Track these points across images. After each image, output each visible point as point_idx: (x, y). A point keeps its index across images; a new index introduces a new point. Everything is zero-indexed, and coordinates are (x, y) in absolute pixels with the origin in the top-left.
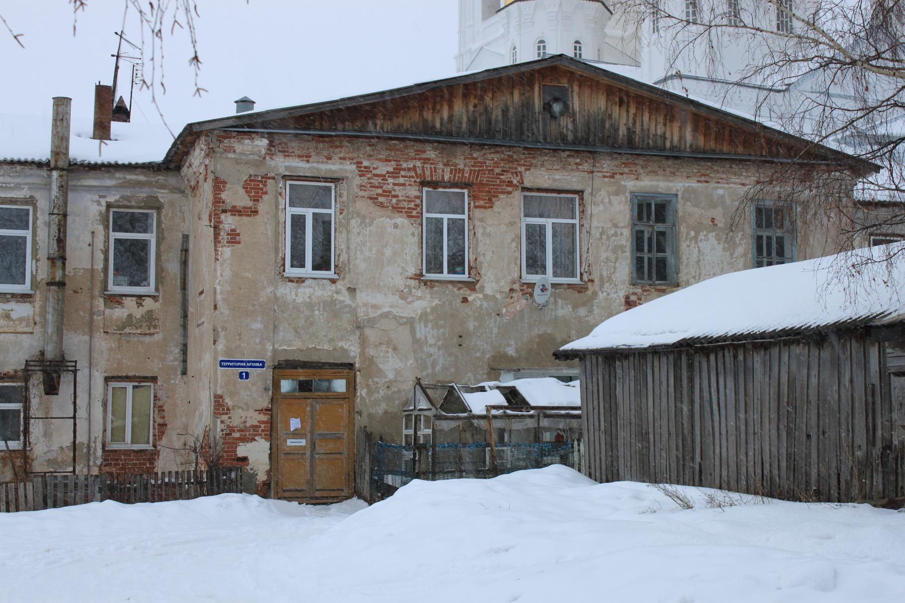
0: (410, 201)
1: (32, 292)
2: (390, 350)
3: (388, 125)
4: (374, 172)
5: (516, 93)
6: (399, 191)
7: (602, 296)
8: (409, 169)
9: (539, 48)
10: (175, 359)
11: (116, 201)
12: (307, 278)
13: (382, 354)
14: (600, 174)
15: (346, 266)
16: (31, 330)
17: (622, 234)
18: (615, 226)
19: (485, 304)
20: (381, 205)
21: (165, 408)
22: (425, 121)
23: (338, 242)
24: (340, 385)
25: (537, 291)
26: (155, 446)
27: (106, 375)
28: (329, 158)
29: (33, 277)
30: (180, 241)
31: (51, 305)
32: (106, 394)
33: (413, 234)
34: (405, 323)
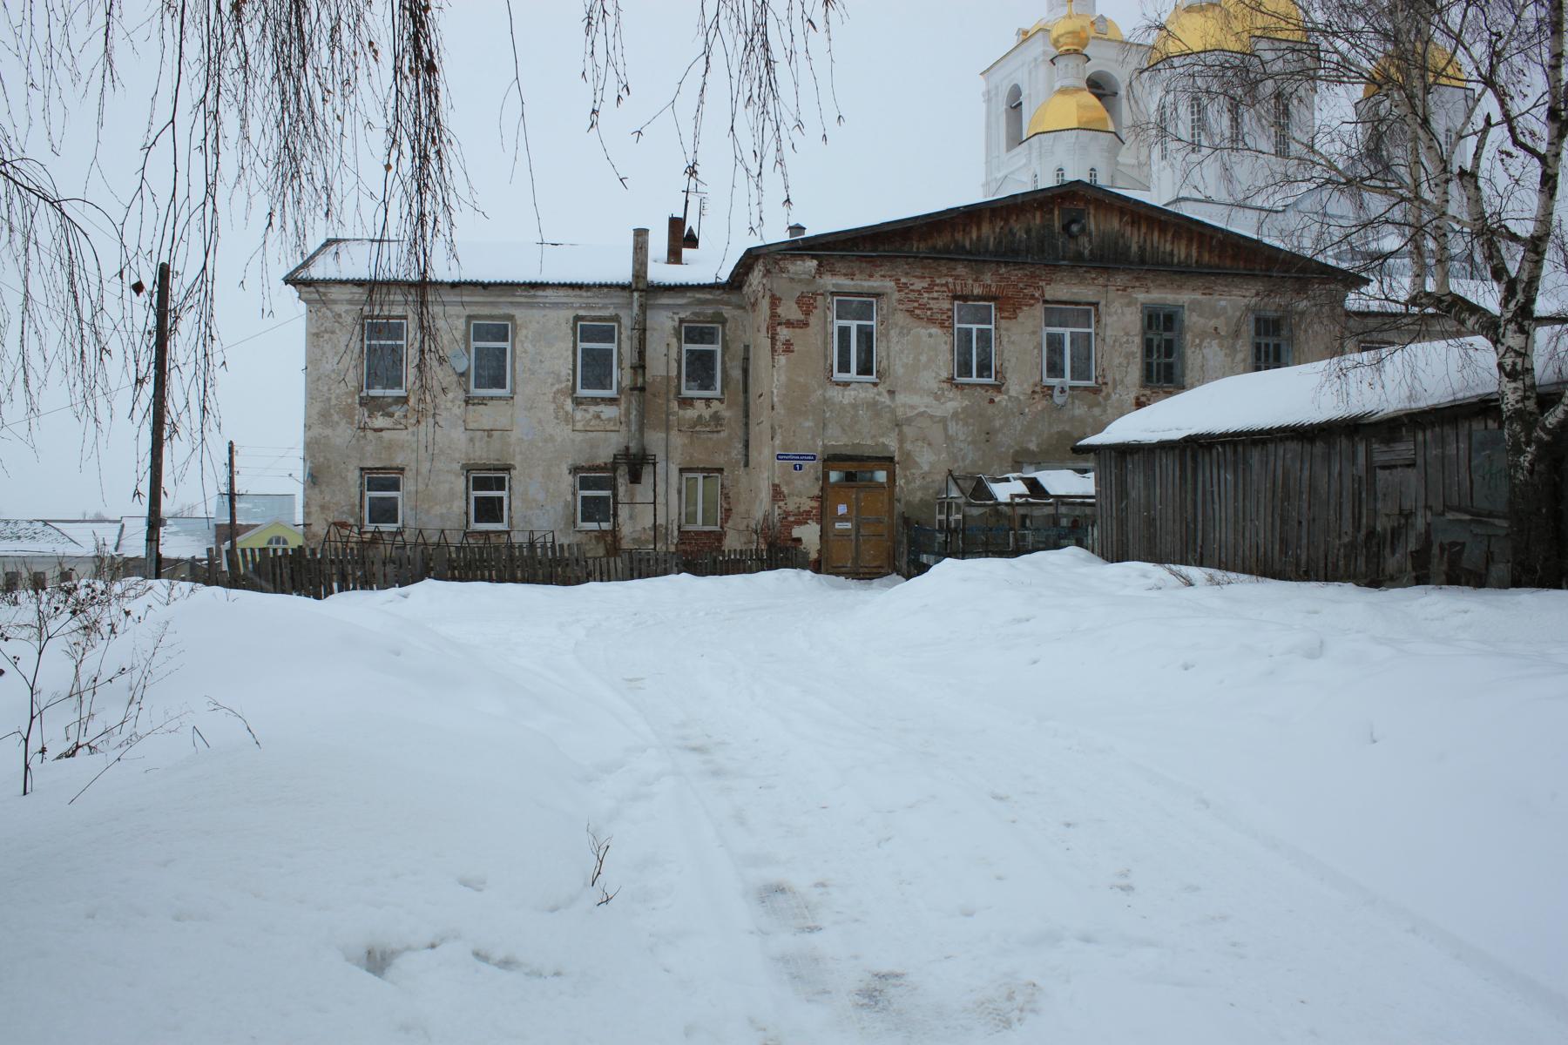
1: (618, 396)
3: (922, 246)
4: (911, 288)
5: (1038, 215)
6: (933, 304)
7: (1114, 397)
8: (942, 285)
9: (1058, 175)
13: (918, 449)
14: (1114, 288)
16: (617, 429)
18: (1127, 334)
19: (1009, 404)
20: (918, 317)
21: (731, 495)
22: (956, 242)
24: (881, 476)
25: (1056, 392)
26: (722, 527)
28: (871, 276)
29: (619, 383)
32: (680, 484)
34: (940, 421)
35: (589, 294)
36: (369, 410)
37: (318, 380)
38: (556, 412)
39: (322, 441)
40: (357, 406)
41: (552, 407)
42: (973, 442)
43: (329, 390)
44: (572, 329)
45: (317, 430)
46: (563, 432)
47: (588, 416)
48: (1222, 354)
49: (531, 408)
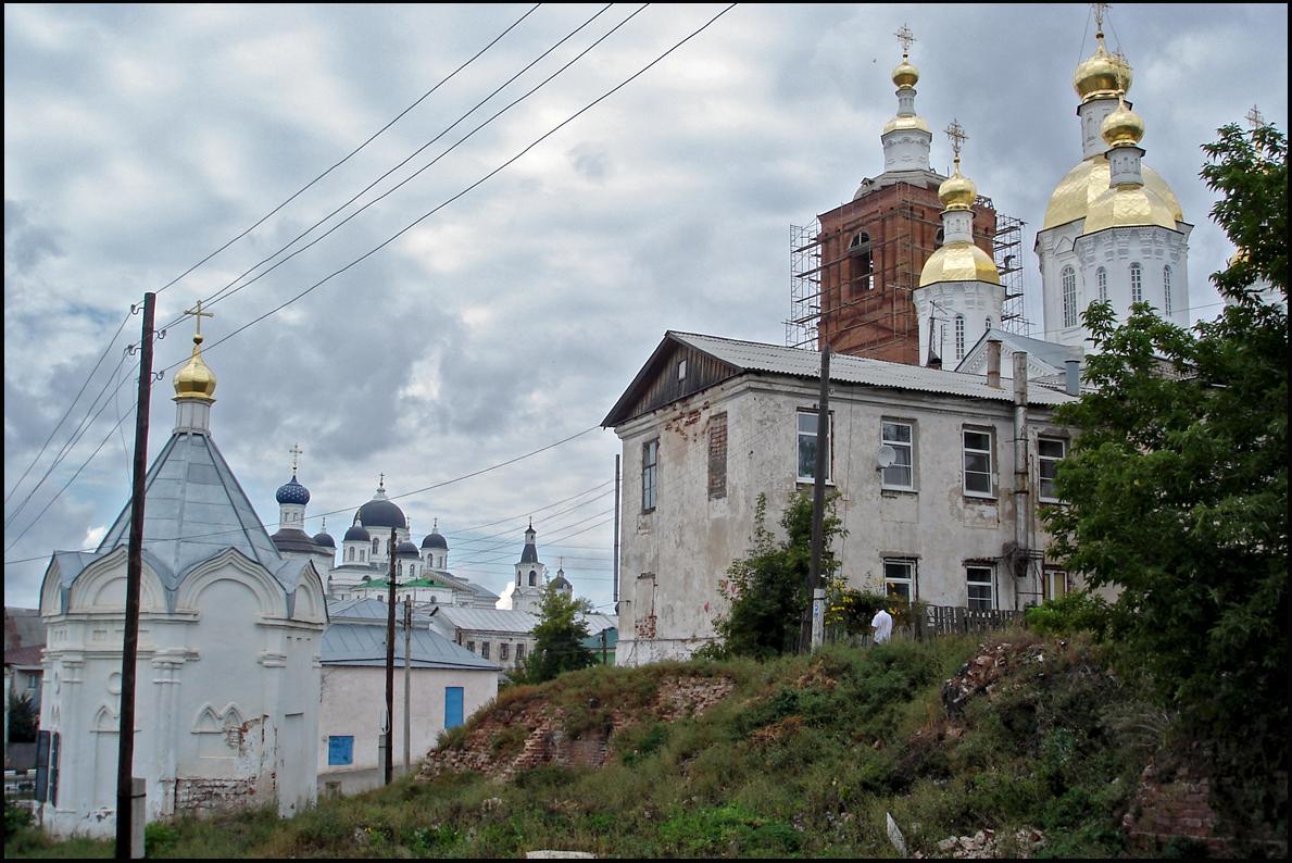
29: (996, 487)
38: (951, 508)
41: (949, 504)
43: (772, 475)
47: (975, 514)
49: (932, 504)
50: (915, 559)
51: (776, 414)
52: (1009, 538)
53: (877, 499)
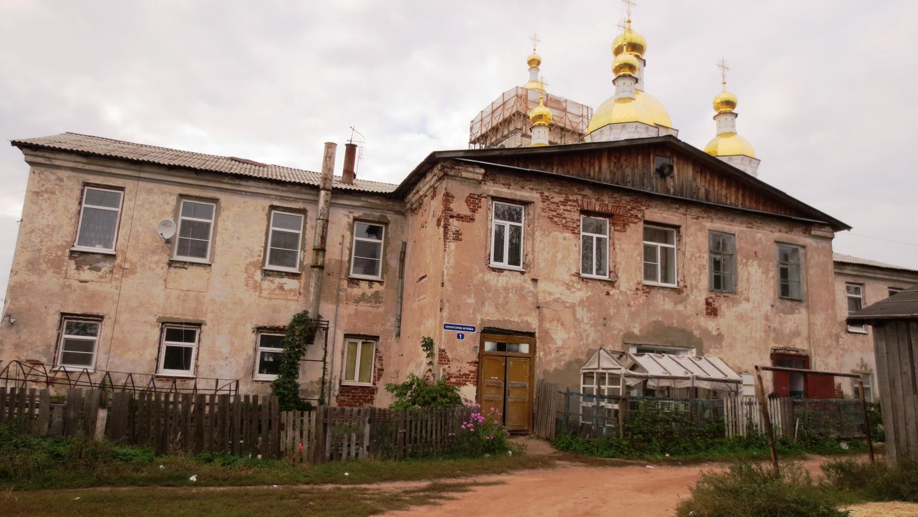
0: (573, 223)
2: (559, 325)
4: (552, 200)
6: (566, 214)
7: (692, 297)
8: (574, 201)
10: (392, 325)
11: (359, 216)
12: (505, 270)
13: (554, 327)
14: (690, 216)
15: (531, 263)
16: (296, 299)
17: (703, 257)
19: (620, 297)
21: (384, 358)
23: (525, 247)
24: (524, 348)
26: (374, 384)
27: (346, 333)
28: (523, 188)
29: (301, 263)
30: (401, 246)
31: (313, 281)
32: (344, 346)
33: (575, 245)
35: (284, 188)
36: (76, 263)
37: (32, 232)
38: (247, 280)
39: (27, 286)
40: (67, 258)
41: (244, 276)
42: (595, 325)
43: (41, 242)
44: (267, 215)
45: (23, 276)
46: (249, 297)
47: (274, 286)
48: (760, 271)
49: (226, 275)
50: (199, 325)
51: (57, 187)
52: (305, 309)
53: (161, 269)
